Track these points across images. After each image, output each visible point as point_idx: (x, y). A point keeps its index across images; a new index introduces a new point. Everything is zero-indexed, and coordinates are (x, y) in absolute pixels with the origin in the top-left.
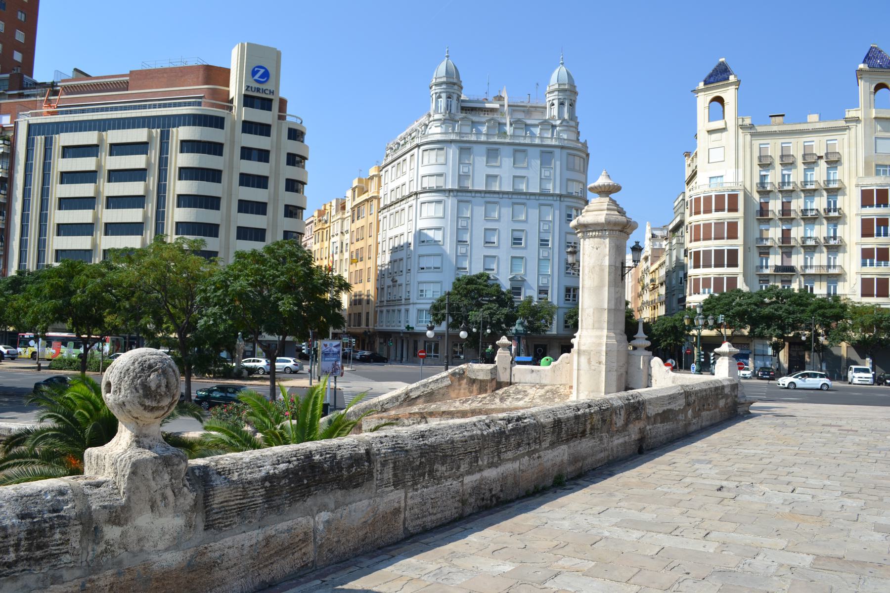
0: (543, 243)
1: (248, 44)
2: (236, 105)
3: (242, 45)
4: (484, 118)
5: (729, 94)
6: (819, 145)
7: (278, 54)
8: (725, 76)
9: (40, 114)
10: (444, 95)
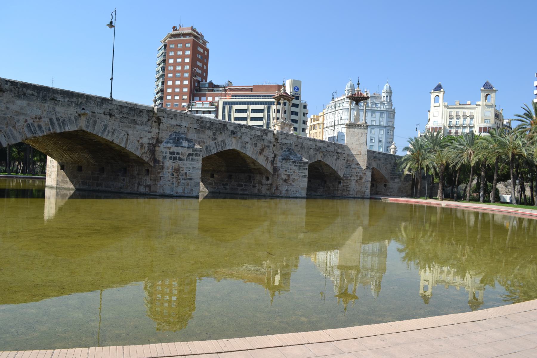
0: (380, 141)
3: (291, 80)
5: (441, 95)
6: (468, 112)
7: (300, 82)
8: (440, 88)
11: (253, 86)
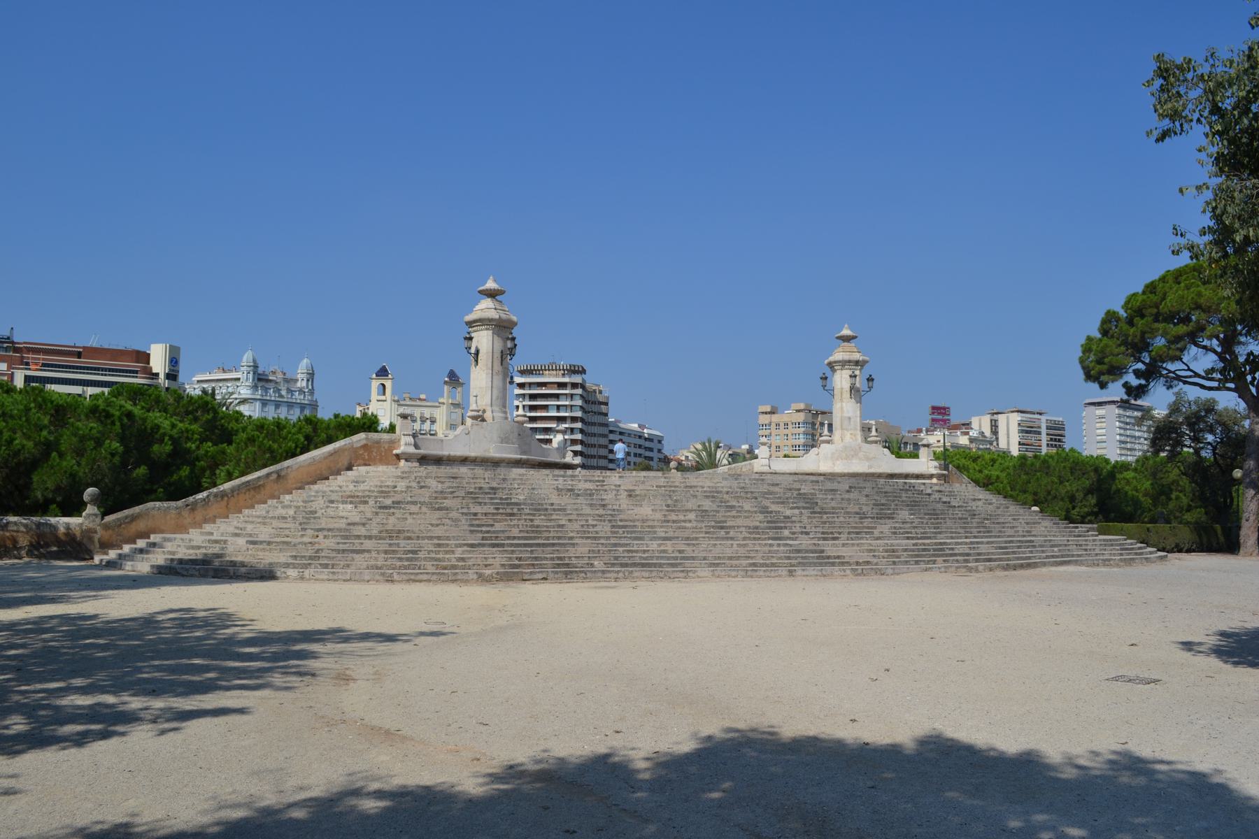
1: (170, 346)
2: (163, 378)
4: (272, 385)
6: (427, 413)
7: (179, 348)
9: (30, 369)
10: (251, 373)
11: (84, 348)
